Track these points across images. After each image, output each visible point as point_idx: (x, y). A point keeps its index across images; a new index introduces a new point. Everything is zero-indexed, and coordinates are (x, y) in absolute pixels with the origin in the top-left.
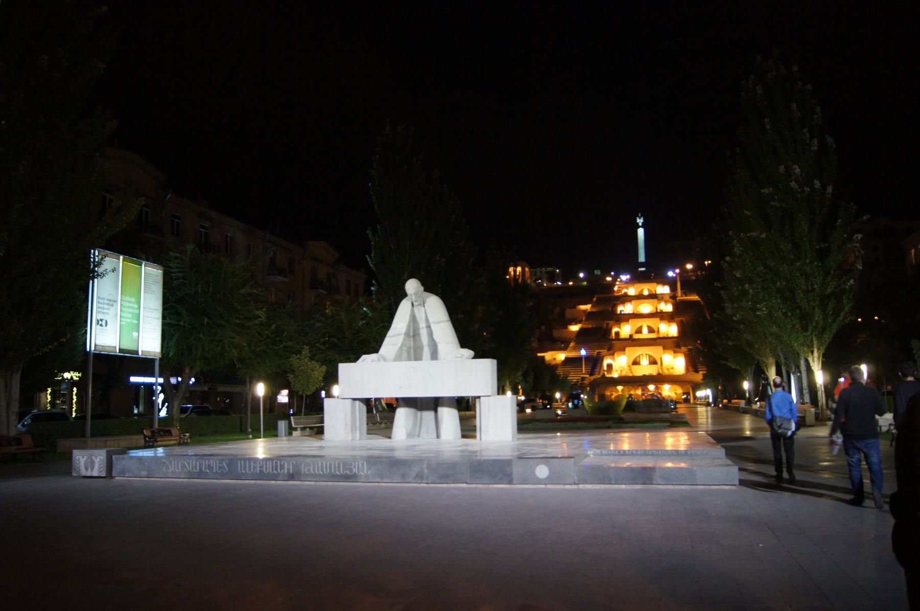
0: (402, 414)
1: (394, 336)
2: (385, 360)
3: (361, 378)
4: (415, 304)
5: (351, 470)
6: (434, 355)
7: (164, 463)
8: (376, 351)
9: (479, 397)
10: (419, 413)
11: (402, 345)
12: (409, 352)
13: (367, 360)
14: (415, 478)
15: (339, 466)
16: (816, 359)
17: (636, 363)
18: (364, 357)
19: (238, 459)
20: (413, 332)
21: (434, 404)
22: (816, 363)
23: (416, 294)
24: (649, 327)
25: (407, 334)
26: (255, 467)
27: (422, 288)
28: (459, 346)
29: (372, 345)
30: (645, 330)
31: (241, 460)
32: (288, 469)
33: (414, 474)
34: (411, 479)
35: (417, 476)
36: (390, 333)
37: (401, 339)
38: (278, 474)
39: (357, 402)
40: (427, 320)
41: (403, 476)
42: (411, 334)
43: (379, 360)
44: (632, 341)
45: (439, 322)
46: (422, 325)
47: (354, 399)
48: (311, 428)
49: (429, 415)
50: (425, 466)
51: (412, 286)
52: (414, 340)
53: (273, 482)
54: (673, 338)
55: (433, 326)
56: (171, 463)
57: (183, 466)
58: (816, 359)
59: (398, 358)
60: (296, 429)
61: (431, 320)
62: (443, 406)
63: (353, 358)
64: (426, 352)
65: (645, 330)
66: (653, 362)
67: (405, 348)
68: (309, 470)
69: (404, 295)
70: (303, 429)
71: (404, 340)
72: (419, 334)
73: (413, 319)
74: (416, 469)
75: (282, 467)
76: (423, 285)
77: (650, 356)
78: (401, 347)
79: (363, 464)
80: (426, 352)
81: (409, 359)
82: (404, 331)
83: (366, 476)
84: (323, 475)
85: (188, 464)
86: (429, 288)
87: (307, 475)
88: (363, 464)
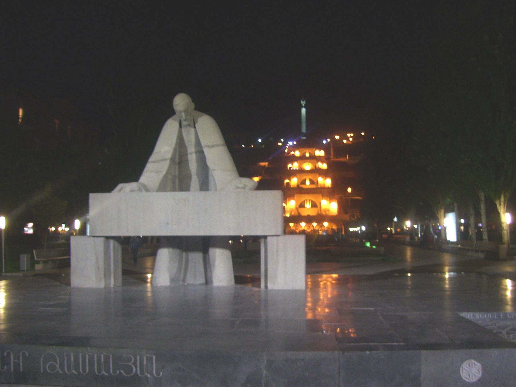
0: (164, 255)
1: (153, 162)
2: (147, 190)
3: (125, 210)
4: (184, 123)
5: (129, 370)
6: (205, 186)
8: (136, 179)
9: (265, 237)
10: (184, 254)
11: (168, 172)
12: (174, 183)
13: (126, 189)
16: (502, 203)
17: (302, 205)
18: (121, 185)
20: (180, 158)
21: (203, 244)
22: (502, 206)
23: (186, 111)
24: (311, 180)
25: (172, 160)
27: (193, 106)
28: (238, 175)
29: (133, 173)
30: (308, 182)
32: (17, 365)
36: (152, 158)
37: (165, 166)
39: (112, 242)
40: (198, 144)
42: (177, 160)
43: (140, 190)
44: (300, 190)
45: (213, 146)
46: (191, 149)
47: (108, 238)
48: (53, 261)
49: (196, 257)
51: (181, 102)
52: (180, 168)
54: (328, 188)
55: (206, 150)
58: (502, 203)
59: (162, 188)
60: (38, 262)
61: (203, 143)
62: (215, 246)
63: (107, 186)
64: (195, 182)
65: (308, 182)
66: (314, 205)
67: (170, 177)
68: (53, 367)
69: (171, 112)
70: (45, 262)
71: (170, 167)
72: (187, 161)
73: (181, 144)
76: (194, 101)
77: (312, 202)
78: (165, 177)
79: (150, 360)
80: (195, 182)
81: (174, 190)
82: (169, 155)
86: (202, 105)
88: (150, 360)
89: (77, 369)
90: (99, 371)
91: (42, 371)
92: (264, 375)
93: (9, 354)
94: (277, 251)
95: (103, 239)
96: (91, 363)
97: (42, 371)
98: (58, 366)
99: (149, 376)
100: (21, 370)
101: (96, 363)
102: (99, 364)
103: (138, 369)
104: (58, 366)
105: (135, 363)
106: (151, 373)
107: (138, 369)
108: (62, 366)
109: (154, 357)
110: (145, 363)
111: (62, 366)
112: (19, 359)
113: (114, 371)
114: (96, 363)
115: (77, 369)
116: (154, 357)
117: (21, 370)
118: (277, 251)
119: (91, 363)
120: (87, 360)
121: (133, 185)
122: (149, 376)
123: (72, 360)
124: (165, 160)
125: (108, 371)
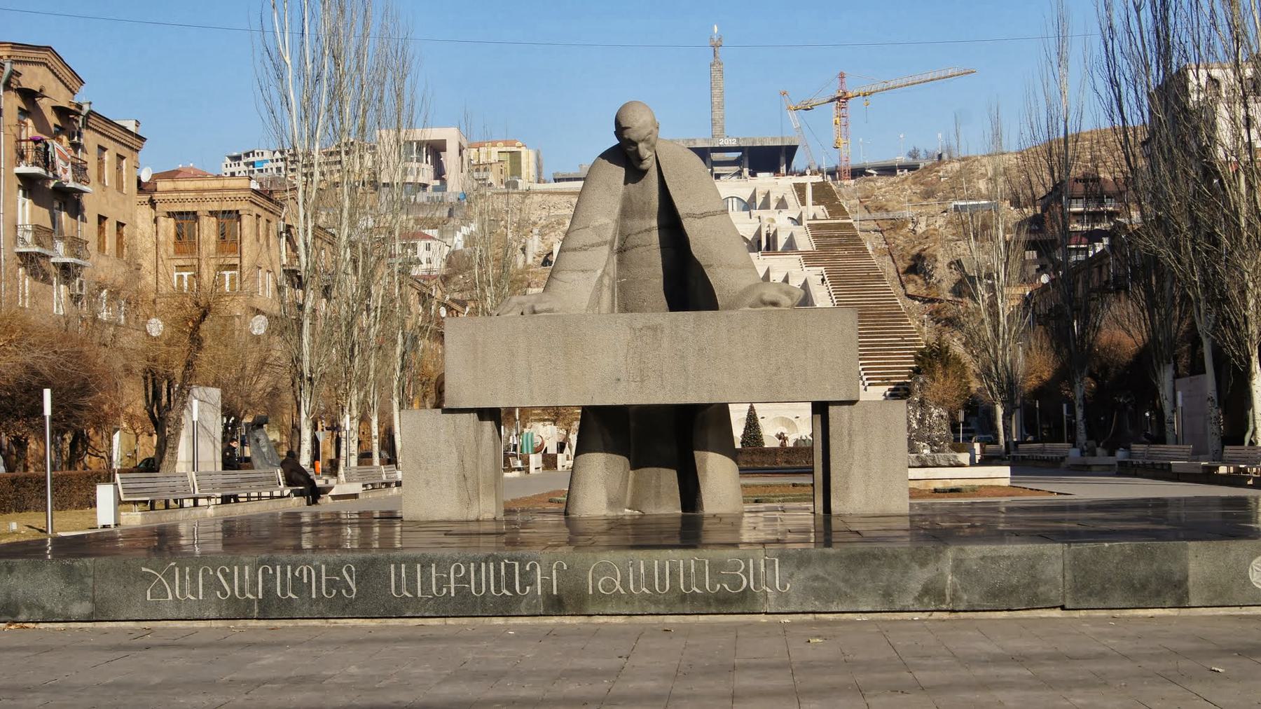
5: (736, 582)
7: (149, 578)
14: (919, 599)
26: (442, 582)
32: (547, 584)
33: (916, 586)
34: (909, 601)
35: (926, 591)
38: (516, 599)
41: (887, 595)
45: (704, 215)
52: (621, 262)
53: (499, 621)
55: (686, 223)
56: (170, 576)
57: (212, 584)
75: (527, 579)
83: (783, 597)
84: (653, 599)
85: (230, 579)
87: (599, 598)
89: (650, 585)
90: (688, 587)
93: (533, 567)
94: (850, 435)
95: (474, 416)
98: (618, 583)
100: (555, 592)
102: (687, 575)
104: (618, 583)
105: (746, 572)
106: (773, 587)
108: (625, 583)
110: (763, 569)
111: (625, 583)
112: (551, 575)
113: (712, 586)
115: (650, 585)
117: (555, 592)
124: (599, 245)
125: (702, 586)
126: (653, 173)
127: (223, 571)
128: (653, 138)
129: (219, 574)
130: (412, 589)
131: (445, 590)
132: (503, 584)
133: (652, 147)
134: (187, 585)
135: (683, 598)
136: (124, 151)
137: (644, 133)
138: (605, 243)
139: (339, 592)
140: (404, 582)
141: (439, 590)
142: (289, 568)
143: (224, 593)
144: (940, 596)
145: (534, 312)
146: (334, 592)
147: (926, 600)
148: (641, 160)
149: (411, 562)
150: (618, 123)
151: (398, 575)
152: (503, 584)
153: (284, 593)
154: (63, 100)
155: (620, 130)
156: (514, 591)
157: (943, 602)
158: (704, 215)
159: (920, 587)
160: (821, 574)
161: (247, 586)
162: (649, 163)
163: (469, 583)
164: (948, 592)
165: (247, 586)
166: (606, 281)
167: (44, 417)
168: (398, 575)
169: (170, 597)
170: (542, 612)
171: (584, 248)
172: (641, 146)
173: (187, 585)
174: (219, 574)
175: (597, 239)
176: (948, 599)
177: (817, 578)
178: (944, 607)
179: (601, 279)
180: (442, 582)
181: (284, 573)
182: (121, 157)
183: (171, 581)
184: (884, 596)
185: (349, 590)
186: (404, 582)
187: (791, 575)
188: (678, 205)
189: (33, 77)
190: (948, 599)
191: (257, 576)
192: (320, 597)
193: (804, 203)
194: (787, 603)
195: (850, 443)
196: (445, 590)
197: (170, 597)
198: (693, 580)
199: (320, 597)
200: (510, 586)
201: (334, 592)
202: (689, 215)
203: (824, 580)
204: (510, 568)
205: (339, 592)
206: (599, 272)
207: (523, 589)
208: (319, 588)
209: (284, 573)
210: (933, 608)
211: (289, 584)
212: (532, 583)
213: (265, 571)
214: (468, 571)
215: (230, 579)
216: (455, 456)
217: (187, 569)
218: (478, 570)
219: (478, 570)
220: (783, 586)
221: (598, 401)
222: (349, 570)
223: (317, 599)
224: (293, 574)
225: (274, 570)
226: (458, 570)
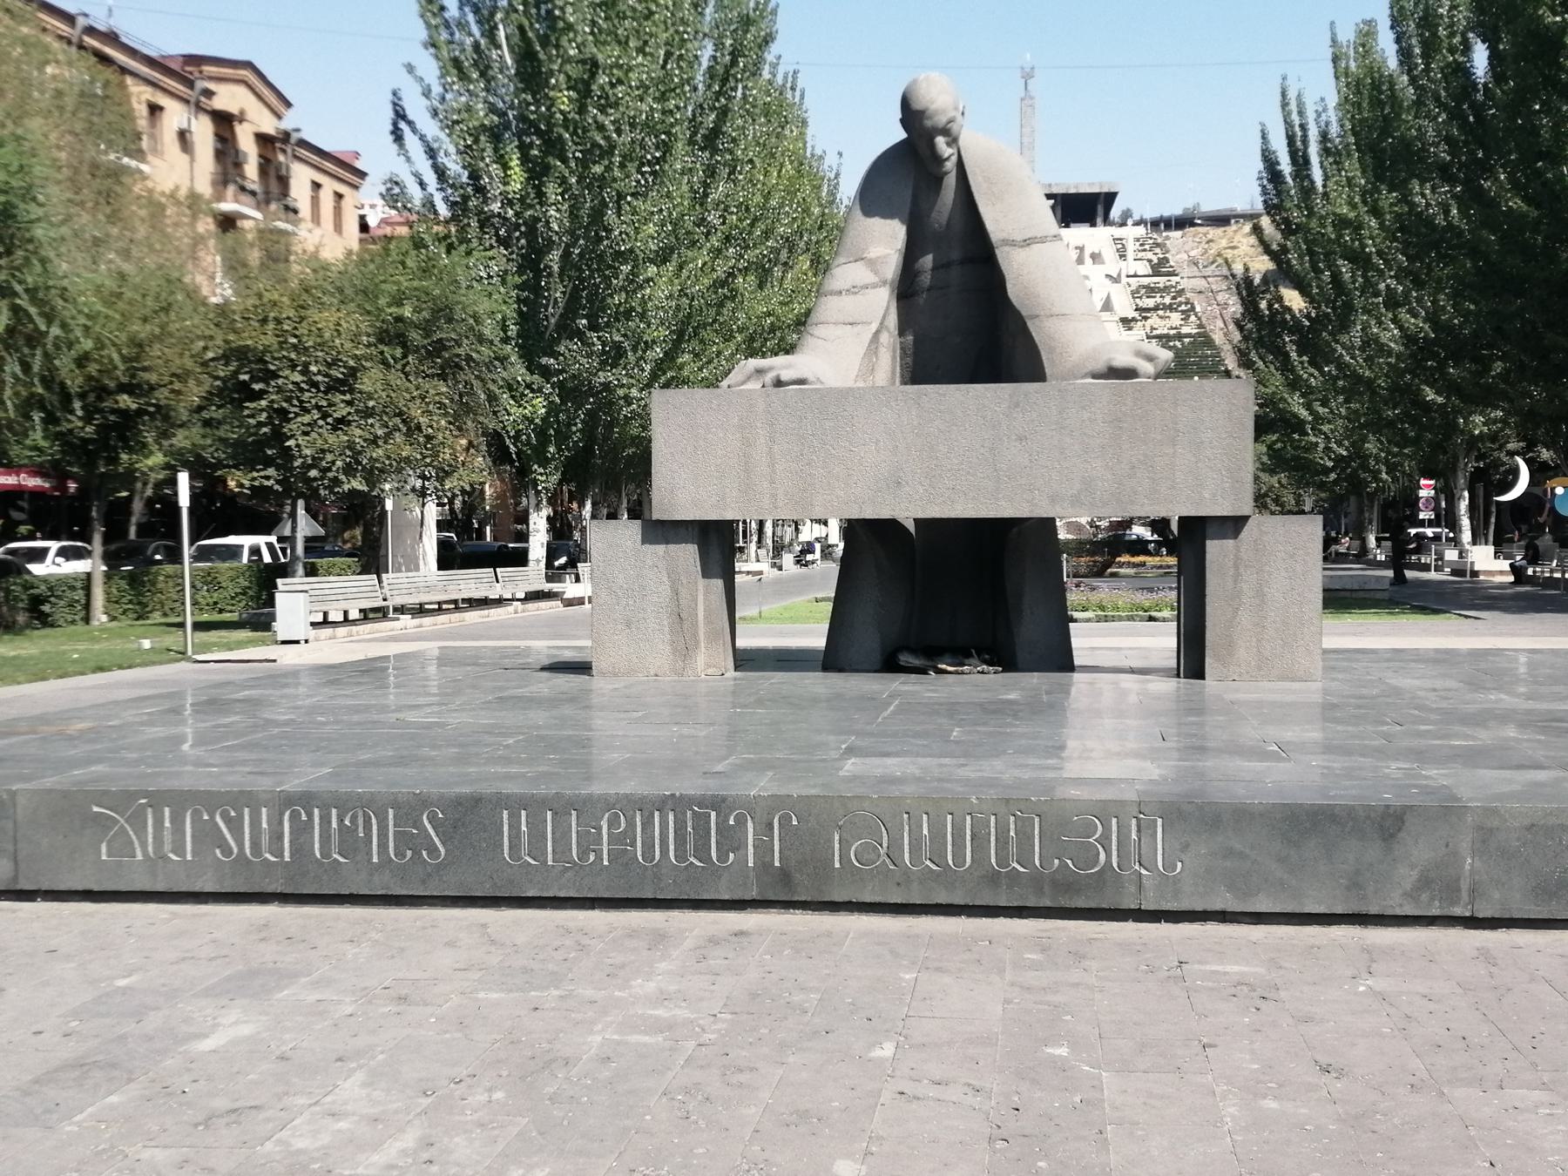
7: (103, 823)
14: (1411, 895)
15: (1025, 837)
19: (502, 801)
26: (589, 843)
31: (516, 804)
32: (763, 849)
33: (1407, 876)
35: (1424, 882)
41: (1355, 885)
50: (1465, 846)
57: (207, 836)
74: (1419, 850)
75: (731, 840)
79: (1144, 828)
83: (1168, 882)
85: (235, 826)
88: (1144, 828)
89: (938, 857)
90: (1003, 860)
91: (837, 865)
92: (1467, 867)
93: (741, 821)
94: (1236, 567)
96: (979, 839)
97: (837, 865)
99: (1144, 872)
100: (777, 864)
101: (993, 838)
103: (1115, 853)
105: (1105, 841)
107: (1115, 853)
109: (1160, 821)
110: (1134, 836)
114: (993, 838)
116: (1160, 821)
117: (777, 864)
118: (1236, 567)
119: (979, 839)
120: (968, 832)
121: (782, 365)
122: (1144, 872)
123: (925, 832)
124: (874, 286)
126: (951, 181)
127: (225, 816)
128: (954, 127)
129: (218, 819)
130: (537, 850)
131: (592, 858)
132: (690, 846)
133: (953, 141)
134: (167, 837)
135: (993, 879)
136: (342, 189)
137: (941, 120)
138: (884, 283)
139: (416, 853)
140: (525, 839)
141: (583, 854)
142: (334, 811)
143: (227, 851)
144: (1451, 890)
145: (779, 383)
146: (409, 853)
147: (1424, 897)
148: (939, 160)
149: (535, 806)
150: (905, 103)
151: (515, 826)
152: (690, 846)
153: (326, 853)
154: (269, 125)
155: (911, 115)
156: (706, 858)
157: (1453, 903)
158: (1028, 242)
159: (1415, 874)
160: (1238, 846)
161: (265, 840)
162: (950, 165)
163: (633, 844)
164: (1465, 886)
165: (265, 840)
166: (885, 338)
167: (176, 509)
168: (515, 826)
169: (140, 857)
170: (753, 894)
171: (853, 290)
172: (940, 141)
173: (167, 837)
174: (218, 819)
175: (870, 278)
176: (1465, 895)
177: (1229, 853)
178: (1457, 911)
179: (878, 332)
180: (589, 843)
181: (325, 820)
182: (339, 196)
183: (141, 830)
184: (1348, 888)
185: (433, 850)
186: (525, 839)
187: (1185, 847)
188: (990, 225)
189: (229, 98)
190: (1465, 895)
191: (281, 823)
192: (385, 861)
193: (1123, 256)
194: (1177, 894)
195: (1237, 577)
196: (592, 858)
197: (140, 857)
198: (1013, 848)
199: (385, 861)
200: (702, 851)
201: (409, 853)
202: (1006, 242)
203: (1242, 856)
204: (702, 823)
205: (416, 853)
206: (874, 327)
207: (723, 857)
208: (383, 846)
209: (325, 820)
210: (1435, 912)
211: (335, 838)
212: (740, 847)
213: (295, 816)
214: (631, 824)
215: (235, 826)
216: (665, 589)
217: (167, 810)
218: (647, 824)
219: (647, 824)
220: (1169, 866)
221: (869, 514)
222: (433, 819)
223: (380, 865)
224: (340, 821)
225: (310, 815)
226: (613, 823)
